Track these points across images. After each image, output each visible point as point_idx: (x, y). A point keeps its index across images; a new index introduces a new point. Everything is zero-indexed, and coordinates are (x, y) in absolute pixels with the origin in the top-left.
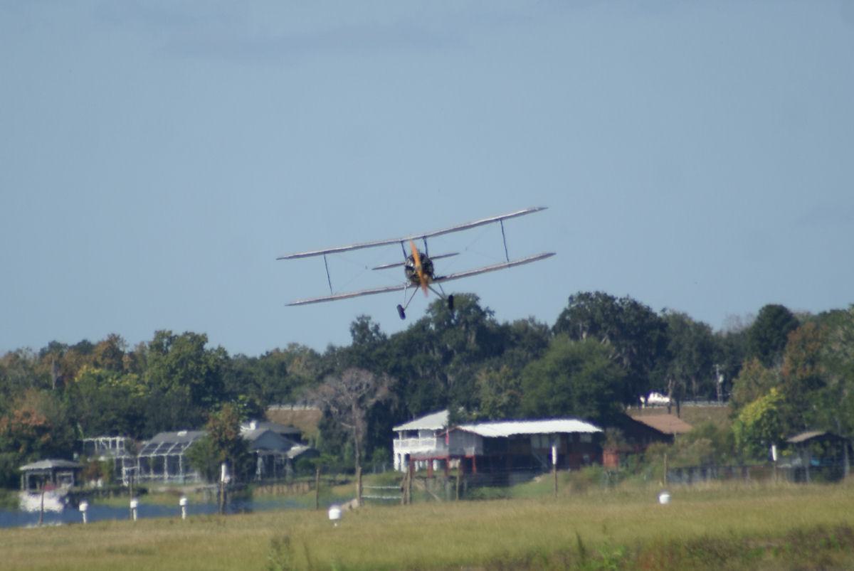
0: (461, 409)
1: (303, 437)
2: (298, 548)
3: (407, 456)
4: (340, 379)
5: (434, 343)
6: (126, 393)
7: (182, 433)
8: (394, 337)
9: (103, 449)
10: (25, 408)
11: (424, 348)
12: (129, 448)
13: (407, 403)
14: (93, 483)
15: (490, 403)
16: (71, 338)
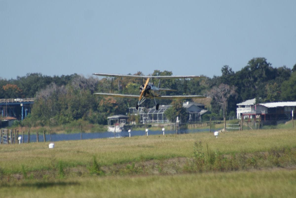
0: (260, 98)
1: (205, 107)
2: (204, 145)
3: (241, 114)
4: (218, 87)
5: (251, 75)
7: (163, 106)
8: (237, 73)
11: (247, 76)
12: (145, 111)
13: (241, 96)
14: (133, 123)
15: (270, 96)
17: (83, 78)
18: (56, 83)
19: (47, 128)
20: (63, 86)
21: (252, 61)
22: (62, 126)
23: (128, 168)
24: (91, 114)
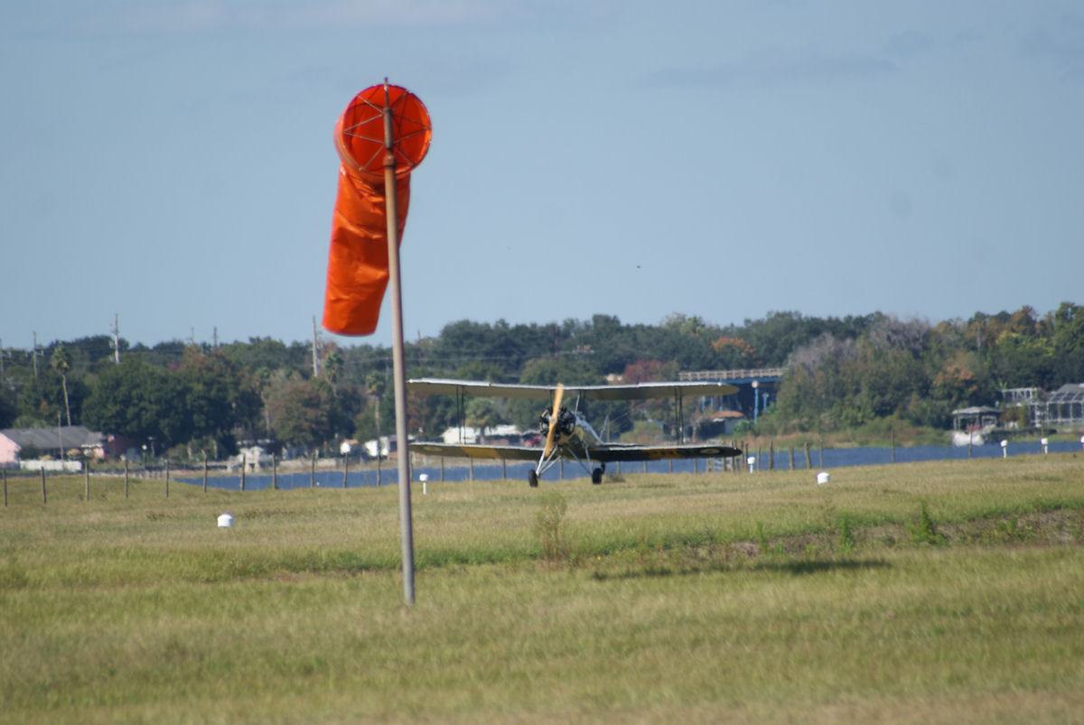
6: (1038, 354)
9: (1020, 399)
10: (957, 366)
12: (1041, 398)
14: (1011, 424)
16: (993, 310)
17: (896, 321)
18: (834, 334)
19: (814, 436)
20: (849, 341)
22: (849, 431)
23: (1003, 528)
24: (915, 404)
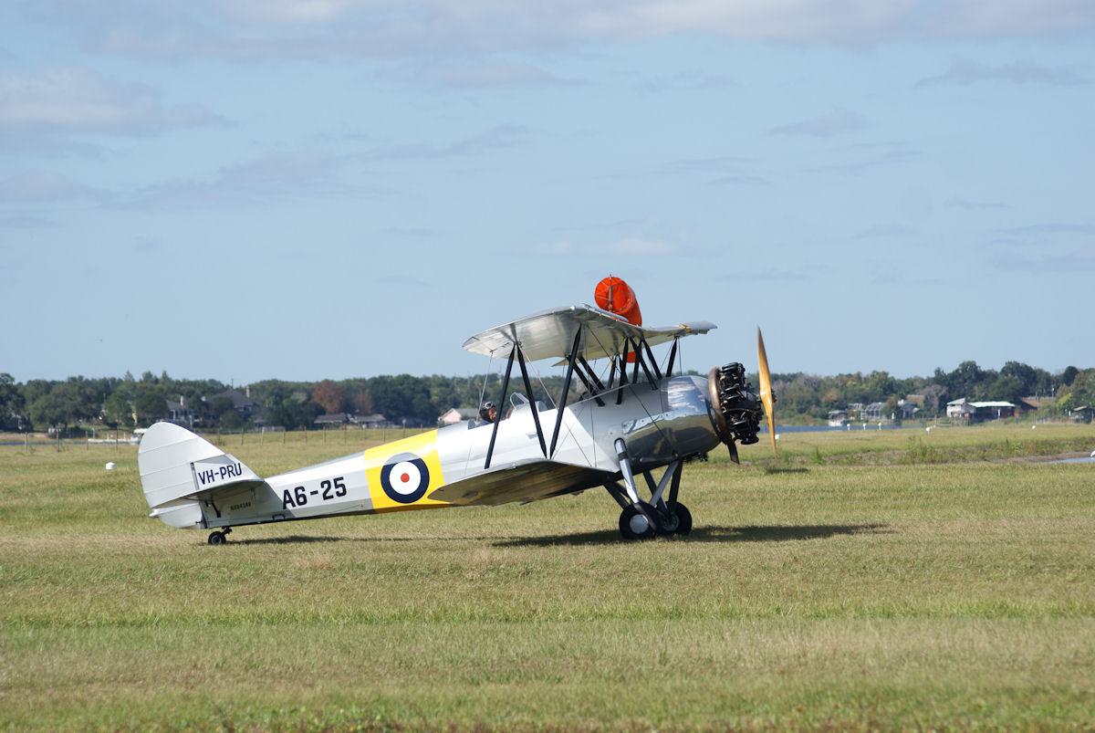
2: (917, 439)
6: (862, 390)
9: (855, 408)
16: (846, 373)
21: (963, 365)
23: (847, 458)
24: (814, 409)
